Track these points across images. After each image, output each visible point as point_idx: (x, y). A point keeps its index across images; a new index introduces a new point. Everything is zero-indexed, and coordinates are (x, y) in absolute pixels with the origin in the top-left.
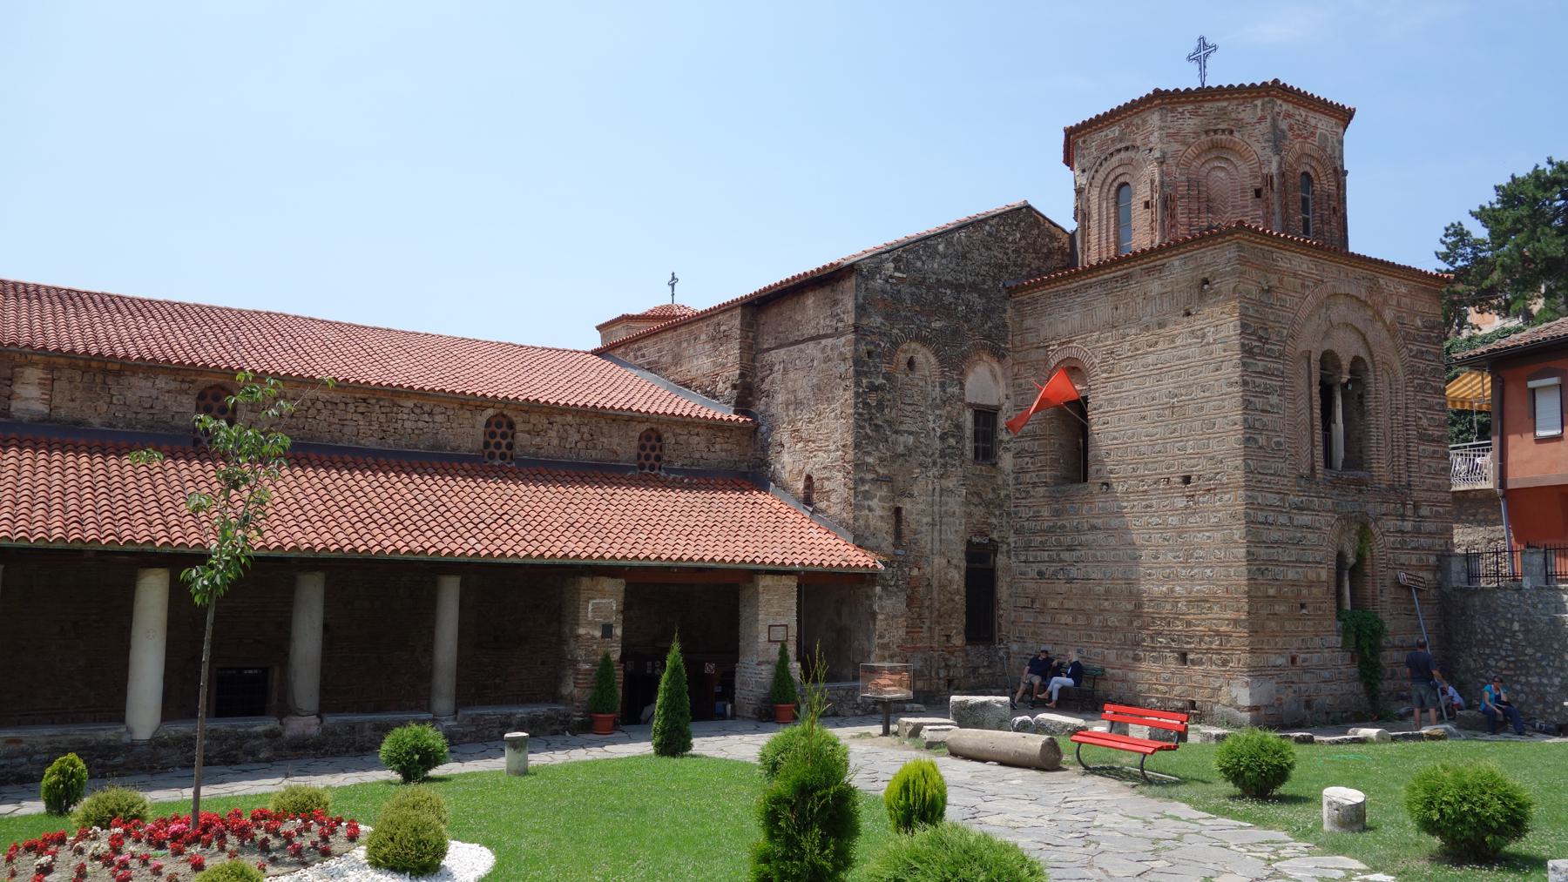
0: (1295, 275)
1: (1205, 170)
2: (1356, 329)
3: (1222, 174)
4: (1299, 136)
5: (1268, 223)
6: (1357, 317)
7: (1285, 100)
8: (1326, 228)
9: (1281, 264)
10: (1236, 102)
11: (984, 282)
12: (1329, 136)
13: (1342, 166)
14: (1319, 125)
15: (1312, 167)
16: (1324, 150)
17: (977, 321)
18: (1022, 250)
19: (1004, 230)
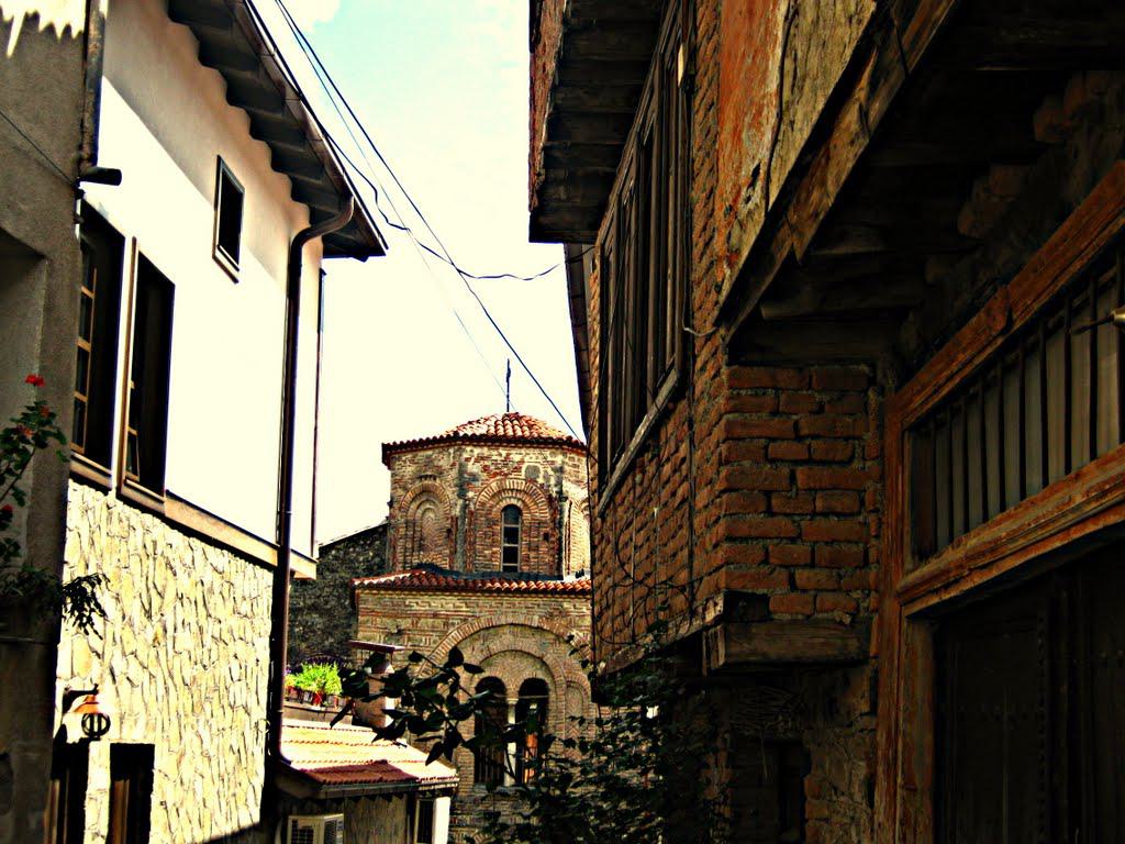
0: (435, 615)
1: (420, 511)
2: (529, 654)
3: (432, 515)
4: (495, 474)
5: (452, 562)
6: (530, 644)
7: (474, 446)
8: (532, 554)
9: (416, 607)
10: (437, 451)
11: (326, 603)
12: (541, 467)
13: (560, 492)
14: (526, 459)
15: (519, 499)
16: (534, 481)
17: (314, 639)
18: (375, 567)
19: (354, 552)
